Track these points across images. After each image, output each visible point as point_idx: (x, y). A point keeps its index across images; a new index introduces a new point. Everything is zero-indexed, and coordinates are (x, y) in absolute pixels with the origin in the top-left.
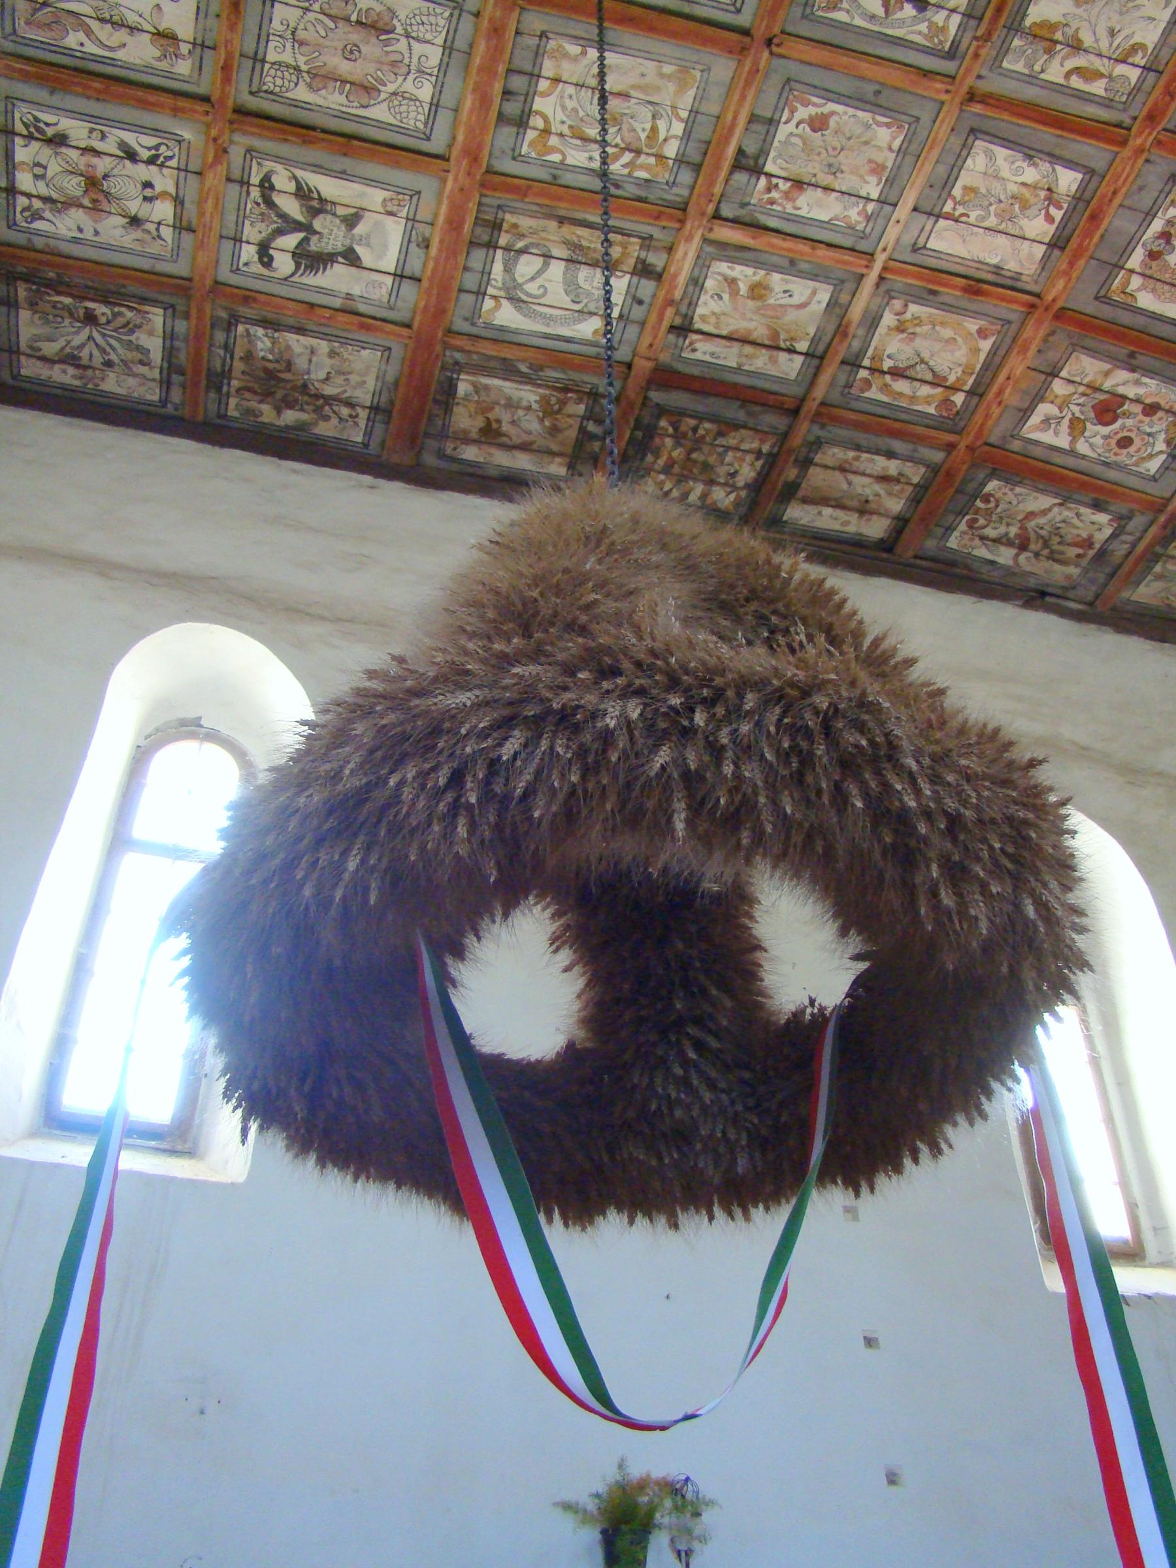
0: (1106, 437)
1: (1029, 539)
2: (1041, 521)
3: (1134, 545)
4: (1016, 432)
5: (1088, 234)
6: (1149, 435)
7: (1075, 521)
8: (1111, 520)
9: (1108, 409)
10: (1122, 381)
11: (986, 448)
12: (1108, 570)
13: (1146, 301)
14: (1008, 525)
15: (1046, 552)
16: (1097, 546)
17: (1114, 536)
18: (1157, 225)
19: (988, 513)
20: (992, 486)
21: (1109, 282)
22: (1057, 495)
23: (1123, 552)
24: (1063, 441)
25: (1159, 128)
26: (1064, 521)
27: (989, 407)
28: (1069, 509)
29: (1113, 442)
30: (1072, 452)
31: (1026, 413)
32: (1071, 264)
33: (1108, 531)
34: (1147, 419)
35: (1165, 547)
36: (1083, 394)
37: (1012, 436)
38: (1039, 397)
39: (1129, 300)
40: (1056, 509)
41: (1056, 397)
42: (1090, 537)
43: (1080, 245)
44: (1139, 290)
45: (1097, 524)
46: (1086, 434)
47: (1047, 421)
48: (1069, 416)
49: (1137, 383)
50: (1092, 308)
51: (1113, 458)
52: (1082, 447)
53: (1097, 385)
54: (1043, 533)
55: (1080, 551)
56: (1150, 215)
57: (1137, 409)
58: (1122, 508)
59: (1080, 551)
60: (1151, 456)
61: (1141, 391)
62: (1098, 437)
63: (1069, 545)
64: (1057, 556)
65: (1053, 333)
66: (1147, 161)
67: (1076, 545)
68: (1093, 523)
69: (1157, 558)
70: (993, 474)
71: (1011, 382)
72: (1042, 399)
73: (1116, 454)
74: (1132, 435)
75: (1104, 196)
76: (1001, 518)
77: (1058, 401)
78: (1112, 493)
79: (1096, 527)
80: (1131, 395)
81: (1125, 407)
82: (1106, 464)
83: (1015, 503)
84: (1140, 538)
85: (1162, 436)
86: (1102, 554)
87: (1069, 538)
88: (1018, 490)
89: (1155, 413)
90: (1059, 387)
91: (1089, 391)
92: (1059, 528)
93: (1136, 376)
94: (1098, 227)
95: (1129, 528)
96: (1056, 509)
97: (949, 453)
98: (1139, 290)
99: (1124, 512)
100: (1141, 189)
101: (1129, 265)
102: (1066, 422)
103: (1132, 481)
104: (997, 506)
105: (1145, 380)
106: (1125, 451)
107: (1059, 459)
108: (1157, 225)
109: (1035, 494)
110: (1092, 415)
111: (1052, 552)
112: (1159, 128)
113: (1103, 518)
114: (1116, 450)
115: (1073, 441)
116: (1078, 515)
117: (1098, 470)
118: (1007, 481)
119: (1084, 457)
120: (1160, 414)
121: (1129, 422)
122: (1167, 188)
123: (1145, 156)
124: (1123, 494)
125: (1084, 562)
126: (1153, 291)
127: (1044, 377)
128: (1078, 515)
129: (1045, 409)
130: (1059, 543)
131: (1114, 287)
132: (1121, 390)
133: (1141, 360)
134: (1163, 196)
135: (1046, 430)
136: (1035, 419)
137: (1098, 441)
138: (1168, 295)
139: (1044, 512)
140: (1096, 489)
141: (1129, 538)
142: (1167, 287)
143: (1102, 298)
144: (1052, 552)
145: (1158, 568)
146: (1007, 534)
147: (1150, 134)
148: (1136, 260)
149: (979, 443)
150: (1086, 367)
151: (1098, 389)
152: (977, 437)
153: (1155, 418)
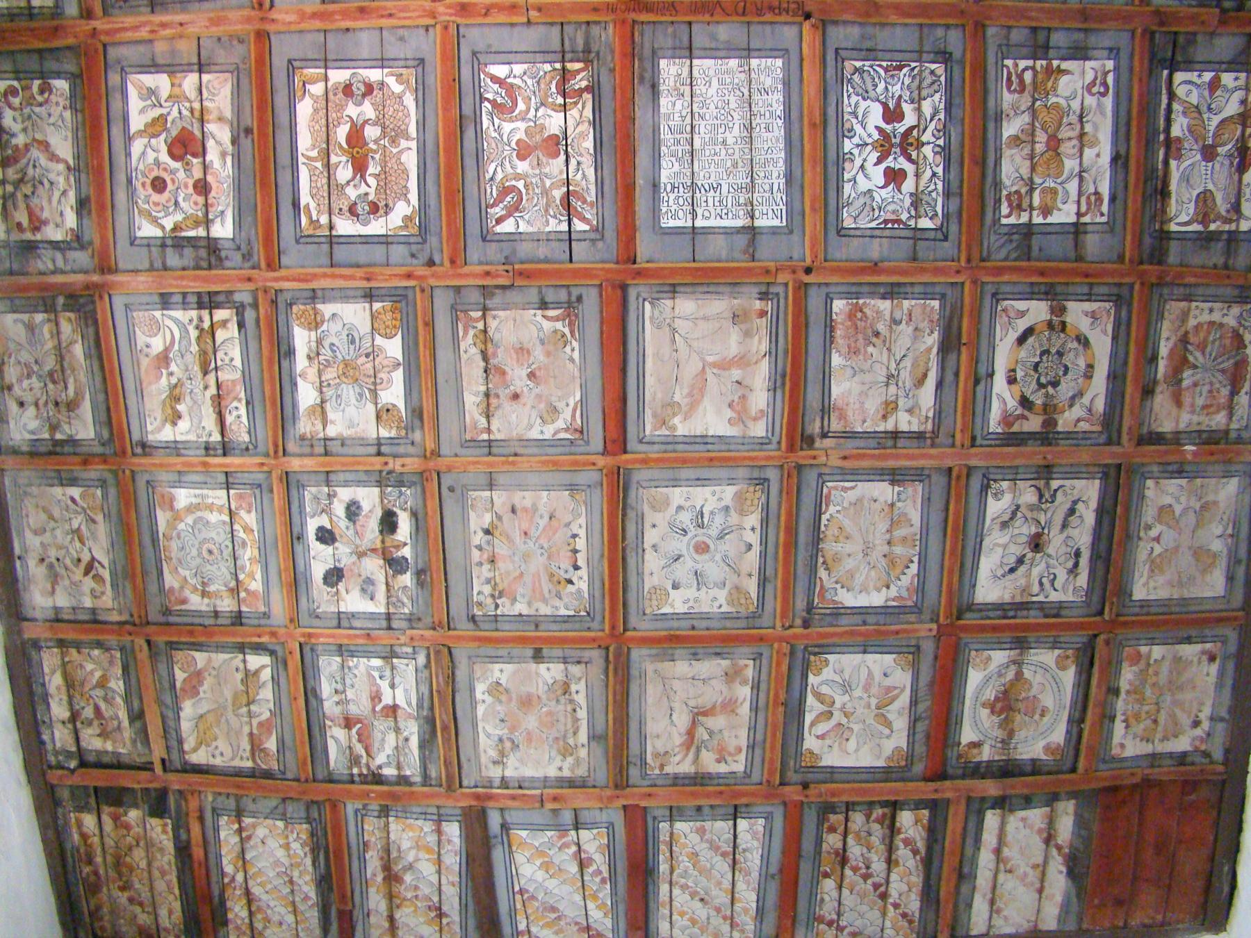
0: (157, 163)
1: (16, 161)
2: (43, 161)
3: (55, 272)
4: (128, 69)
5: (345, 14)
6: (176, 203)
7: (57, 194)
8: (72, 230)
9: (186, 146)
10: (219, 135)
11: (101, 48)
12: (16, 267)
13: (304, 109)
14: (25, 130)
15: (10, 188)
16: (39, 237)
17: (55, 245)
18: (374, 75)
19: (30, 101)
20: (61, 85)
21: (309, 63)
22: (77, 157)
23: (40, 266)
24: (137, 122)
25: (459, 20)
26: (52, 183)
27: (144, 24)
28: (68, 179)
29: (155, 173)
30: (128, 139)
31: (153, 67)
32: (314, 15)
33: (58, 236)
34: (191, 190)
35: (67, 308)
36: (192, 111)
37: (122, 69)
38: (172, 69)
39: (299, 94)
40: (61, 167)
41: (180, 86)
42: (45, 223)
43: (333, 13)
44: (312, 96)
45: (62, 217)
46: (153, 141)
47: (152, 92)
48: (164, 111)
49: (223, 155)
50: (279, 63)
51: (138, 185)
52: (137, 147)
53: (206, 118)
54: (30, 171)
55: (25, 223)
56: (382, 62)
57: (198, 174)
58: (91, 233)
59: (25, 223)
60: (155, 221)
61: (217, 164)
62: (155, 155)
63: (28, 207)
64: (10, 203)
65: (241, 41)
66: (427, 28)
67: (31, 214)
68: (62, 214)
69: (50, 308)
70: (74, 78)
71: (179, 29)
72: (171, 74)
73: (143, 185)
74: (170, 187)
75: (385, 8)
76: (29, 117)
77: (177, 90)
78: (102, 207)
79: (59, 220)
80: (208, 158)
81: (195, 161)
82: (130, 181)
83: (52, 120)
84: (63, 272)
85: (179, 217)
86: (30, 248)
87: (35, 201)
88: (68, 114)
89: (198, 193)
90: (190, 82)
91: (197, 114)
92: (42, 184)
93: (230, 148)
94: (355, 19)
95: (72, 255)
96: (61, 167)
97: (82, 17)
98: (312, 96)
99: (86, 238)
100: (402, 39)
101: (330, 72)
102: (157, 112)
103: (122, 220)
104: (41, 105)
105: (229, 160)
106: (150, 191)
107: (116, 131)
108: (374, 75)
109: (70, 135)
110: (174, 133)
111: (13, 195)
112: (459, 20)
113: (71, 220)
114: (148, 182)
115: (140, 133)
116: (64, 193)
117: (121, 178)
118: (73, 96)
119: (128, 155)
120: (201, 200)
121: (181, 175)
122: (410, 63)
123: (432, 22)
124: (106, 220)
125: (16, 236)
126: (316, 111)
127: (195, 60)
128: (64, 193)
129: (161, 82)
130: (26, 196)
131: (306, 71)
132: (210, 144)
133: (246, 143)
134: (402, 63)
135: (144, 99)
136: (148, 80)
137: (151, 156)
138: (317, 127)
139: (54, 158)
140: (100, 188)
141: (60, 263)
142: (324, 121)
143: (292, 67)
144: (13, 195)
145: (39, 317)
146: (13, 135)
147: (451, 15)
148: (338, 76)
149: (103, 38)
150: (220, 94)
151: (202, 121)
152: (108, 33)
153: (195, 197)
